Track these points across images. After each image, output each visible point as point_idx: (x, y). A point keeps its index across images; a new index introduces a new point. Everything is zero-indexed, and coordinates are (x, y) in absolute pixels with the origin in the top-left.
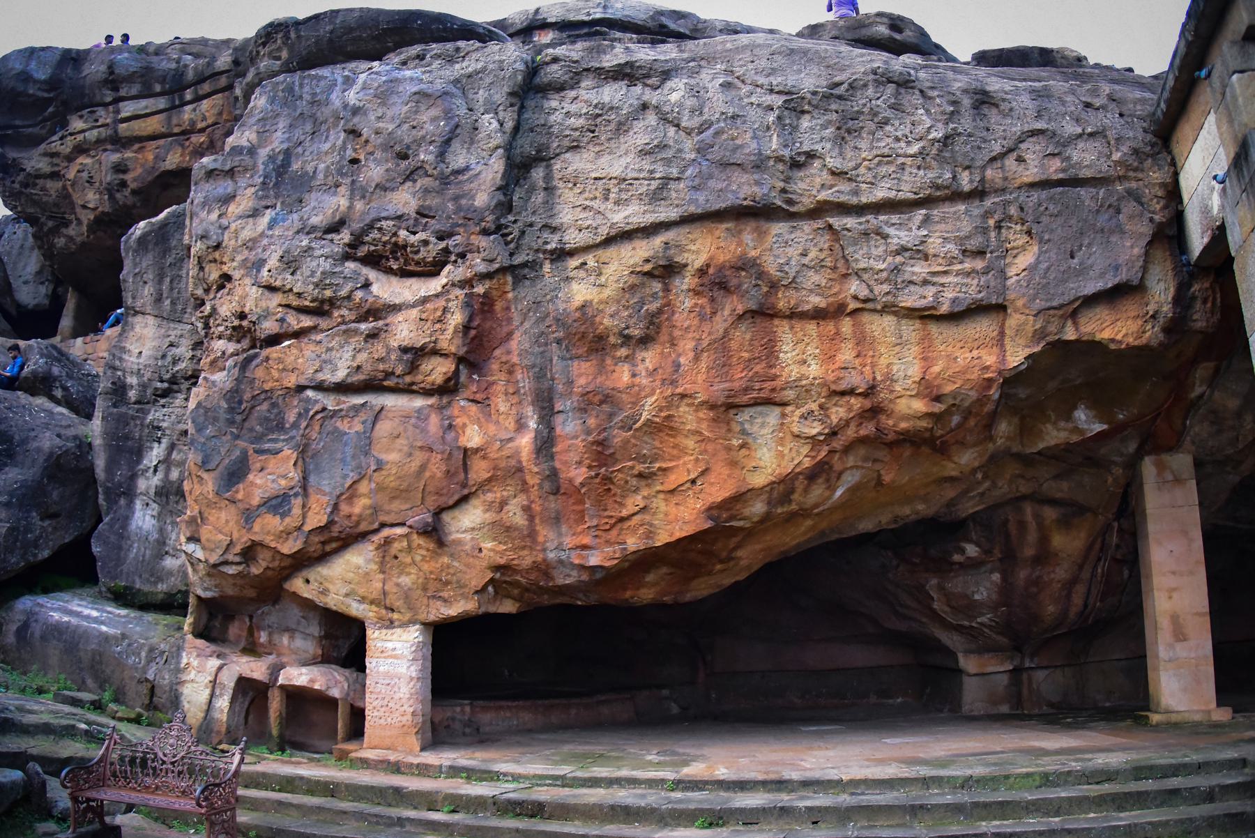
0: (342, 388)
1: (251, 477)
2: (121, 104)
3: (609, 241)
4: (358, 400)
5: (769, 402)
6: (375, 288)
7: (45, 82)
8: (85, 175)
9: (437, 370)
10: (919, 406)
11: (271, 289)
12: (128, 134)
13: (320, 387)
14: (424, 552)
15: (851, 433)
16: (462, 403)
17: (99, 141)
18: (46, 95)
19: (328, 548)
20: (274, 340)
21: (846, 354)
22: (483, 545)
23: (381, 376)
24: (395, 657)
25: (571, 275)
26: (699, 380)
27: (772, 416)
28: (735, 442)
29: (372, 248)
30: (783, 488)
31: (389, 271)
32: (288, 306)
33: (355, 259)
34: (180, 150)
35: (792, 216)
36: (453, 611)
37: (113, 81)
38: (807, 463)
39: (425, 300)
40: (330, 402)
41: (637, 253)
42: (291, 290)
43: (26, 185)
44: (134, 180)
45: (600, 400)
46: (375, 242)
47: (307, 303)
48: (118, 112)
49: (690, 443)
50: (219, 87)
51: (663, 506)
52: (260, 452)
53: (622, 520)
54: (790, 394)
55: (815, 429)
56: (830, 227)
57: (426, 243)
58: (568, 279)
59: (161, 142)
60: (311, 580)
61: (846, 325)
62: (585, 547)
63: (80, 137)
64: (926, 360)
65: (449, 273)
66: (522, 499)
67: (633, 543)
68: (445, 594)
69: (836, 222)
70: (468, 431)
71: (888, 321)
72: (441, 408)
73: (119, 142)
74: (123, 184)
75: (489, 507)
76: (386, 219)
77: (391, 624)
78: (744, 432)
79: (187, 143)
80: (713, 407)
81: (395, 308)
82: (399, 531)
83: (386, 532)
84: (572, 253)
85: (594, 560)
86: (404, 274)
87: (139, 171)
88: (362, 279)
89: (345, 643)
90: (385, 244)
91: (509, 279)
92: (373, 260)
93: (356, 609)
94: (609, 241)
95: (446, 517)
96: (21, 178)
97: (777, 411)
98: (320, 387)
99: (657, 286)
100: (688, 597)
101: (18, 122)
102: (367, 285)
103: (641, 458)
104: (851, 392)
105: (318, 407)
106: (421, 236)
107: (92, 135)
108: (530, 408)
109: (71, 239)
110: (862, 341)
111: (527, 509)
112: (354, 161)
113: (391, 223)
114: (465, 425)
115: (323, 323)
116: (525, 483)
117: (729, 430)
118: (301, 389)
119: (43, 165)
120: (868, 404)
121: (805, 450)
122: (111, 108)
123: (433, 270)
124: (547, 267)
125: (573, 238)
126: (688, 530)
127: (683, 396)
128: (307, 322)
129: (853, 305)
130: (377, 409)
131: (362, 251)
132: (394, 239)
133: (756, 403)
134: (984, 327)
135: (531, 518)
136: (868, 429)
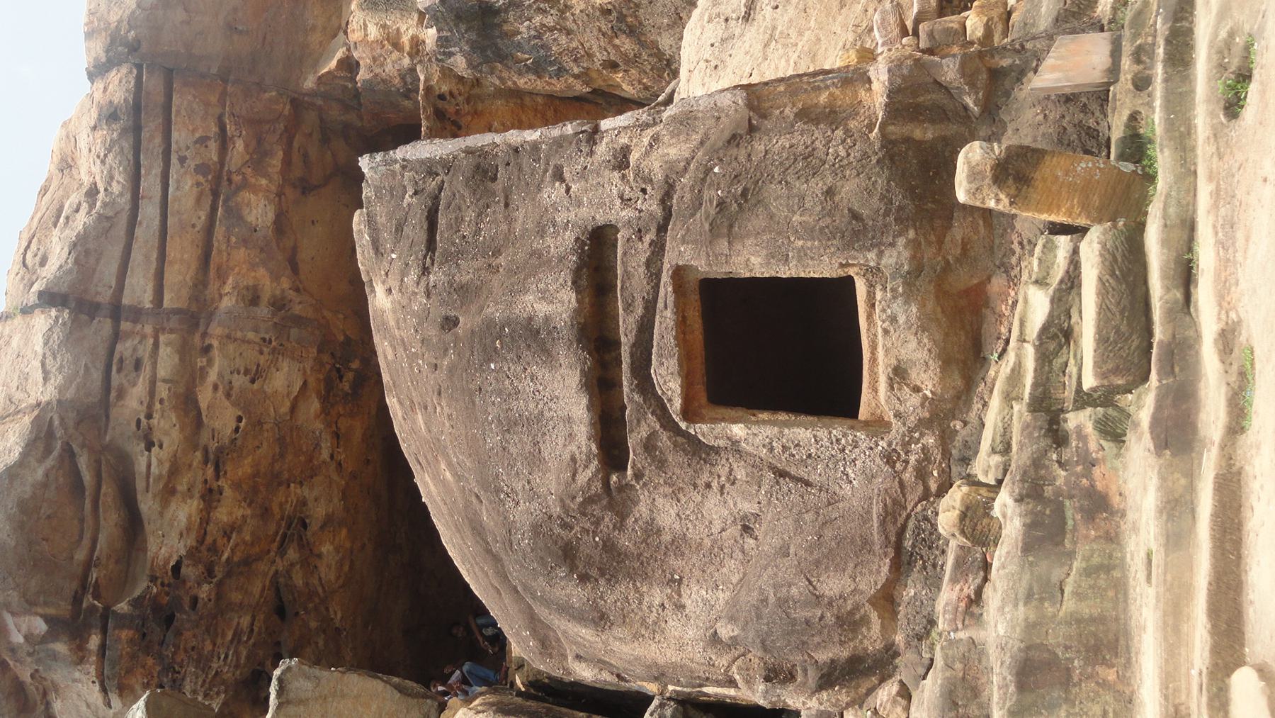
2: (126, 301)
8: (239, 381)
12: (185, 293)
17: (184, 350)
18: (56, 453)
34: (246, 195)
43: (210, 572)
44: (276, 278)
48: (137, 314)
50: (160, 99)
63: (163, 391)
73: (194, 317)
74: (279, 304)
79: (237, 178)
87: (261, 271)
96: (188, 571)
107: (167, 362)
109: (328, 521)
119: (184, 511)
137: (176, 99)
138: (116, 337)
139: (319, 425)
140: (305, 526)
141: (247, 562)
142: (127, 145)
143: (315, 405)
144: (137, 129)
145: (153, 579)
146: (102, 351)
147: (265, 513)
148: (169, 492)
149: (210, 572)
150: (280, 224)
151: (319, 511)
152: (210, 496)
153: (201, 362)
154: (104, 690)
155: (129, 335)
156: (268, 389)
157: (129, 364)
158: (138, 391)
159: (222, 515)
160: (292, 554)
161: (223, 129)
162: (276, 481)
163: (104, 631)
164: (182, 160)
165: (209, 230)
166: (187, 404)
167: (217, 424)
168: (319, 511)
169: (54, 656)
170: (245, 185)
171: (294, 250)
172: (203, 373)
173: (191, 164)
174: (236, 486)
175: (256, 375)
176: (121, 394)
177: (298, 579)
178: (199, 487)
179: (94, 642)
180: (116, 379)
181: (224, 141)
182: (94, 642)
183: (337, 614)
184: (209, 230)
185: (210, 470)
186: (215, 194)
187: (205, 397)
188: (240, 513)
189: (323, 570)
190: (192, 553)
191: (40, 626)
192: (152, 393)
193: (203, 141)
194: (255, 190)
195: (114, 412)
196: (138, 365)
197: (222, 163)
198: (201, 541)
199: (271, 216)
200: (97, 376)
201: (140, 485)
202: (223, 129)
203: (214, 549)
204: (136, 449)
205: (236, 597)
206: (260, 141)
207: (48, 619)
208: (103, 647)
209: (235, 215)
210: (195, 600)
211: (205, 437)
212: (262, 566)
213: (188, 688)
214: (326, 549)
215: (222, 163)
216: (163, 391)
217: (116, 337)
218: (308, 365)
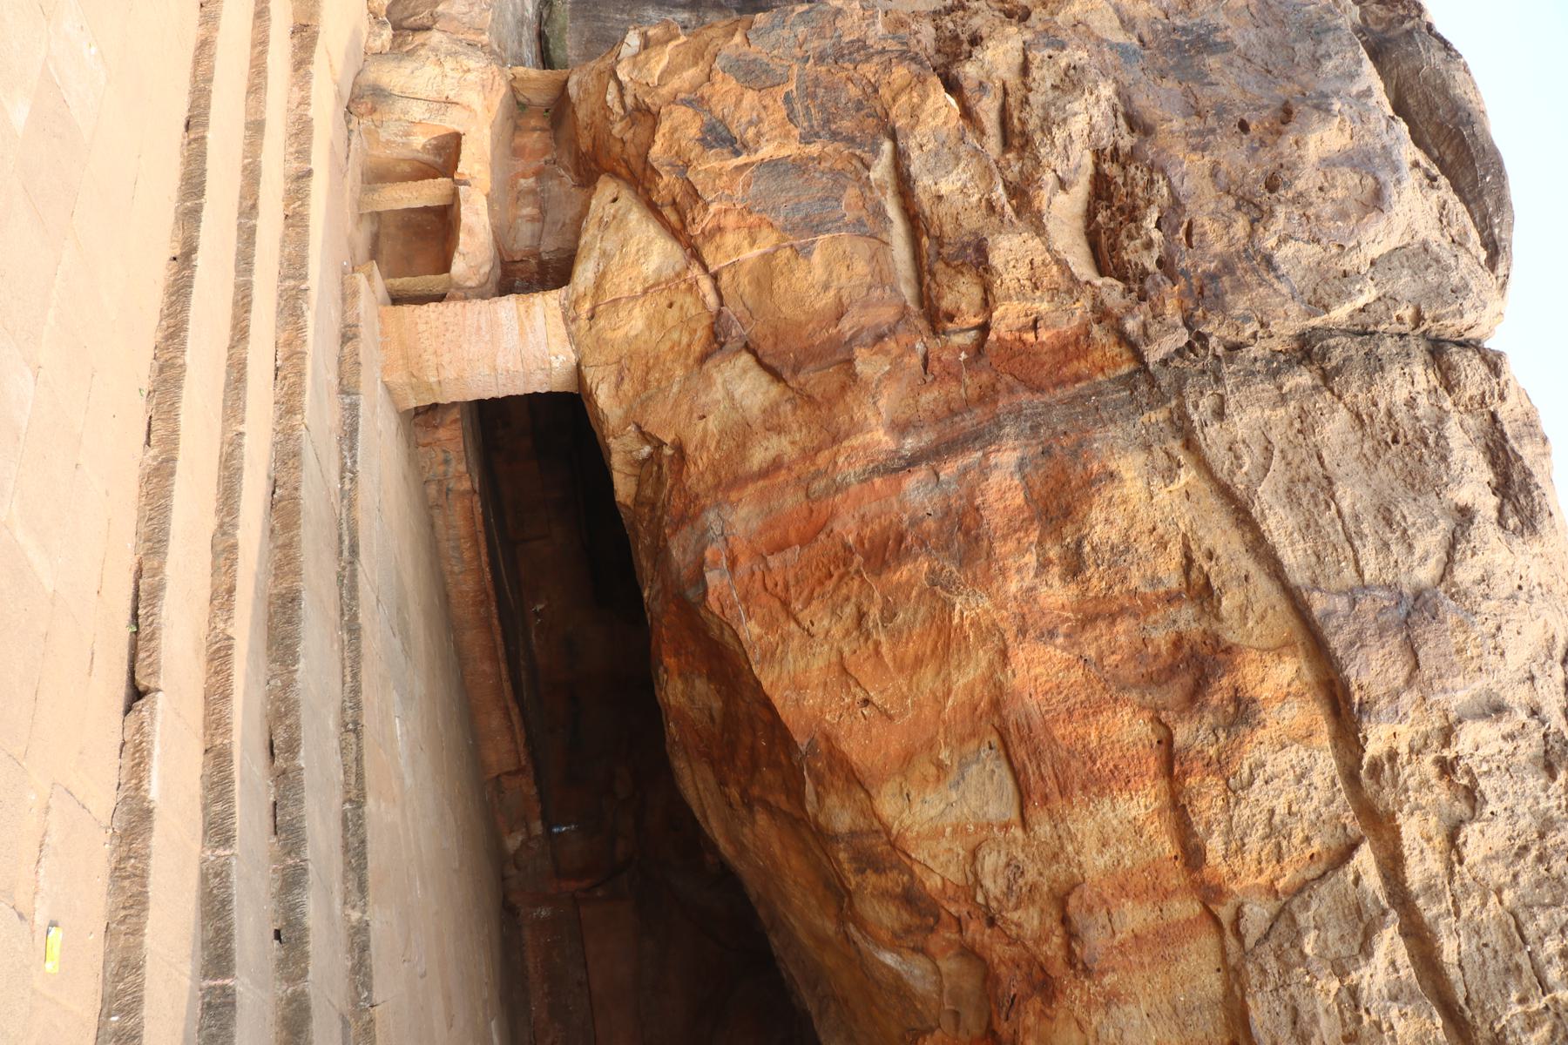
0: (904, 184)
3: (1225, 492)
4: (892, 210)
5: (1023, 795)
6: (1061, 198)
9: (961, 294)
11: (1025, 69)
13: (899, 157)
14: (685, 340)
15: (1000, 951)
16: (919, 346)
19: (668, 212)
20: (952, 86)
21: (1134, 916)
22: (711, 418)
23: (934, 231)
24: (522, 334)
25: (1156, 447)
26: (1039, 670)
27: (1000, 805)
28: (944, 755)
29: (1120, 181)
30: (882, 851)
31: (1090, 214)
32: (1005, 93)
33: (1097, 165)
35: (1351, 777)
38: (933, 883)
40: (880, 170)
41: (1221, 537)
42: (1030, 90)
45: (964, 535)
46: (1130, 182)
47: (1016, 114)
49: (928, 679)
51: (818, 663)
52: (788, 99)
53: (785, 604)
54: (1044, 830)
55: (993, 886)
56: (1352, 847)
57: (1149, 245)
58: (1148, 447)
60: (618, 204)
61: (1185, 908)
62: (733, 562)
65: (1112, 291)
67: (751, 630)
68: (626, 386)
69: (1365, 858)
70: (880, 358)
71: (1212, 984)
72: (904, 312)
75: (771, 411)
76: (1170, 185)
77: (569, 319)
78: (963, 765)
80: (996, 705)
81: (1039, 229)
82: (711, 299)
83: (706, 285)
84: (1190, 444)
85: (714, 579)
88: (1069, 177)
89: (533, 271)
90: (1130, 194)
91: (1125, 369)
92: (1101, 188)
93: (584, 274)
94: (1225, 492)
95: (745, 359)
97: (1014, 815)
98: (899, 157)
99: (1172, 578)
100: (680, 764)
102: (1063, 184)
103: (889, 615)
104: (1072, 937)
105: (867, 156)
106: (1156, 235)
108: (933, 436)
110: (1162, 941)
111: (776, 465)
112: (1244, 126)
113: (1165, 191)
114: (887, 353)
115: (993, 144)
116: (818, 450)
117: (962, 741)
118: (893, 136)
120: (1058, 968)
121: (954, 874)
124: (1159, 415)
125: (1213, 437)
126: (787, 713)
127: (1004, 654)
128: (990, 119)
129: (1225, 913)
130: (885, 237)
131: (1109, 168)
132: (1142, 204)
133: (1017, 774)
135: (764, 473)
136: (1012, 982)
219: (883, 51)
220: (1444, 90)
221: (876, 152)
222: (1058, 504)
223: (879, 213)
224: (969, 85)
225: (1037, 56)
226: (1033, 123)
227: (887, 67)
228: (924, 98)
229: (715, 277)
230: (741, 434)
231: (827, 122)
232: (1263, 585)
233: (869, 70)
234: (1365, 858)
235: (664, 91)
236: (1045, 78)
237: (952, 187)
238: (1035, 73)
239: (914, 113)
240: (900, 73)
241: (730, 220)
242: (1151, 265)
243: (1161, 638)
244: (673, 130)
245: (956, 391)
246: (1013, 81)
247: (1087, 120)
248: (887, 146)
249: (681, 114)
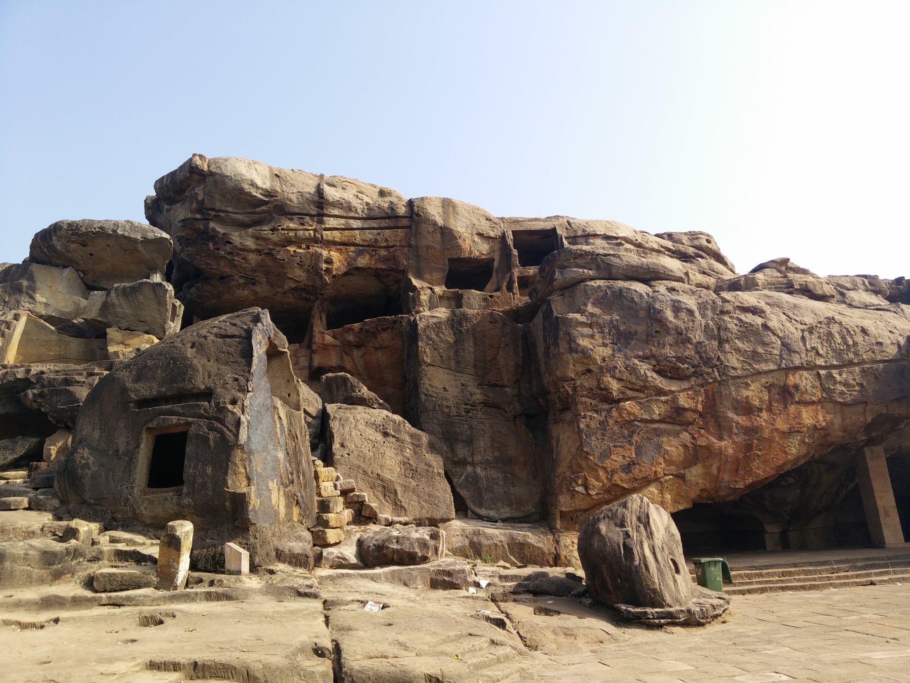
0: (653, 421)
1: (613, 457)
2: (325, 218)
3: (753, 375)
7: (266, 190)
8: (298, 259)
9: (690, 416)
10: (840, 434)
11: (619, 380)
20: (619, 401)
30: (798, 459)
34: (367, 257)
36: (681, 508)
37: (322, 203)
39: (684, 390)
48: (321, 222)
50: (400, 225)
56: (818, 374)
59: (352, 248)
62: (736, 481)
63: (291, 234)
64: (843, 419)
66: (718, 464)
67: (750, 481)
86: (671, 378)
94: (753, 375)
101: (229, 209)
106: (686, 366)
109: (255, 293)
115: (641, 395)
119: (250, 243)
121: (805, 447)
122: (316, 219)
123: (686, 378)
127: (777, 429)
128: (636, 394)
134: (860, 408)
137: (400, 230)
138: (311, 216)
139: (286, 287)
140: (254, 284)
141: (235, 266)
142: (383, 215)
143: (293, 286)
144: (389, 218)
145: (224, 234)
146: (305, 212)
147: (254, 271)
148: (257, 238)
149: (230, 253)
150: (358, 269)
151: (258, 289)
152: (258, 251)
153: (304, 246)
154: (183, 220)
155: (313, 220)
156: (296, 270)
157: (302, 221)
158: (292, 225)
159: (251, 256)
160: (241, 281)
161: (392, 247)
162: (267, 274)
163: (202, 219)
164: (379, 234)
165: (354, 245)
166: (290, 242)
167: (282, 253)
168: (258, 289)
169: (192, 203)
170: (372, 256)
171: (352, 274)
172: (300, 247)
173: (379, 238)
174: (263, 260)
175: (301, 265)
176: (291, 220)
177: (233, 283)
178: (259, 247)
179: (198, 216)
180: (295, 217)
181: (387, 248)
182: (198, 216)
183: (226, 297)
184: (354, 245)
185: (266, 251)
186: (368, 246)
187: (292, 249)
188: (253, 262)
189: (239, 291)
190: (236, 247)
191: (200, 198)
192: (291, 230)
193: (386, 240)
194: (370, 260)
195: (283, 217)
196: (302, 224)
197: (380, 247)
198: (241, 250)
199: (360, 266)
200: (297, 210)
201: (258, 228)
202: (392, 247)
203: (238, 254)
204: (270, 226)
205: (222, 263)
206: (389, 260)
207: (203, 200)
208: (197, 219)
209: (360, 253)
210: (219, 249)
211: (278, 249)
212: (234, 271)
213: (189, 248)
214: (246, 292)
215: (380, 247)
216: (291, 234)
217: (311, 216)
218: (306, 282)
219: (606, 417)
220: (632, 266)
221: (638, 427)
222: (747, 409)
223: (655, 429)
224: (621, 396)
225: (618, 375)
226: (642, 384)
227: (612, 417)
228: (626, 410)
229: (665, 475)
230: (707, 475)
231: (624, 437)
232: (774, 374)
233: (611, 422)
234: (822, 372)
235: (605, 481)
236: (626, 376)
237: (658, 410)
238: (624, 378)
239: (629, 413)
240: (614, 413)
241: (654, 469)
242: (693, 370)
243: (777, 397)
244: (622, 480)
245: (712, 423)
246: (623, 384)
247: (644, 368)
248: (636, 423)
249: (616, 477)
